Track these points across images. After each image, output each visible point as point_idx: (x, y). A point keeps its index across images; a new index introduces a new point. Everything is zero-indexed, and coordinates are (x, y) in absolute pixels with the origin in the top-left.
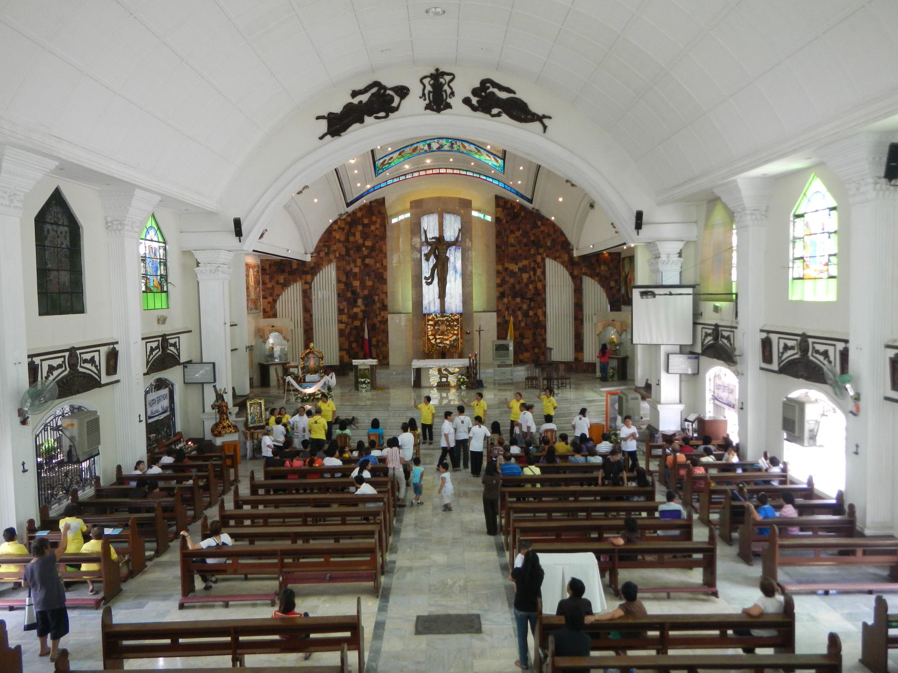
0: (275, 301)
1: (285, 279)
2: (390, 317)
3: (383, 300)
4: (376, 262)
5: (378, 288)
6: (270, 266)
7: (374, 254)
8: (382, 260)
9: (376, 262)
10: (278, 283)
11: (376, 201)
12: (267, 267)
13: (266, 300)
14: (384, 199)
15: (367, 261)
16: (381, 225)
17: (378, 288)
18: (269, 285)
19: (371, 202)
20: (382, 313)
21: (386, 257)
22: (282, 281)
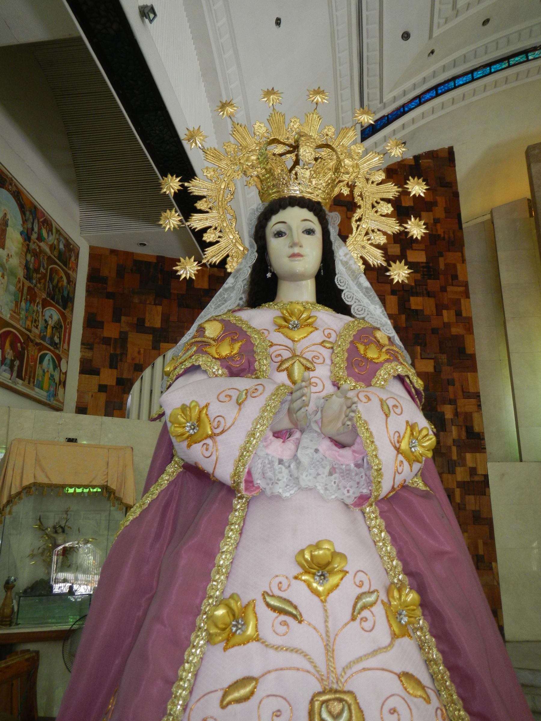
0: (125, 385)
1: (165, 319)
2: (494, 470)
3: (468, 417)
4: (440, 308)
5: (451, 382)
6: (121, 271)
7: (433, 285)
8: (457, 303)
9: (440, 308)
10: (140, 326)
11: (431, 155)
12: (108, 271)
13: (94, 381)
14: (451, 151)
15: (416, 303)
16: (447, 211)
17: (451, 382)
18: (111, 331)
19: (417, 158)
20: (468, 456)
21: (467, 295)
22: (155, 318)
